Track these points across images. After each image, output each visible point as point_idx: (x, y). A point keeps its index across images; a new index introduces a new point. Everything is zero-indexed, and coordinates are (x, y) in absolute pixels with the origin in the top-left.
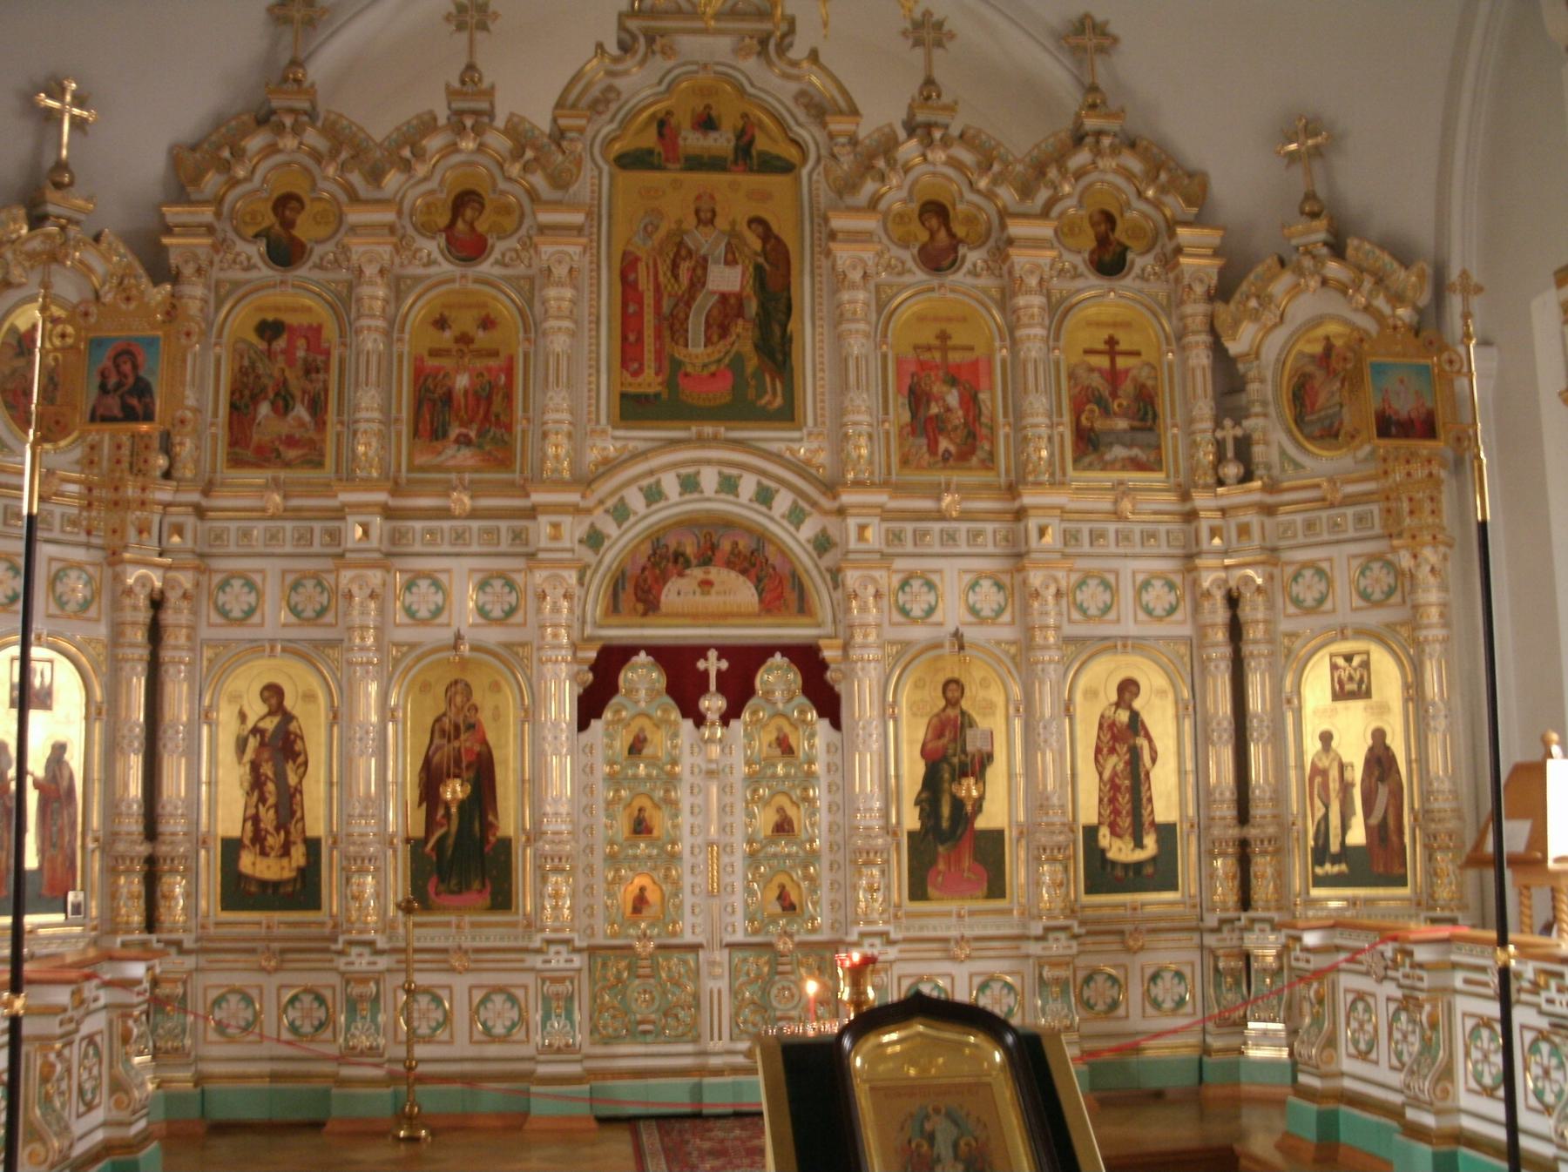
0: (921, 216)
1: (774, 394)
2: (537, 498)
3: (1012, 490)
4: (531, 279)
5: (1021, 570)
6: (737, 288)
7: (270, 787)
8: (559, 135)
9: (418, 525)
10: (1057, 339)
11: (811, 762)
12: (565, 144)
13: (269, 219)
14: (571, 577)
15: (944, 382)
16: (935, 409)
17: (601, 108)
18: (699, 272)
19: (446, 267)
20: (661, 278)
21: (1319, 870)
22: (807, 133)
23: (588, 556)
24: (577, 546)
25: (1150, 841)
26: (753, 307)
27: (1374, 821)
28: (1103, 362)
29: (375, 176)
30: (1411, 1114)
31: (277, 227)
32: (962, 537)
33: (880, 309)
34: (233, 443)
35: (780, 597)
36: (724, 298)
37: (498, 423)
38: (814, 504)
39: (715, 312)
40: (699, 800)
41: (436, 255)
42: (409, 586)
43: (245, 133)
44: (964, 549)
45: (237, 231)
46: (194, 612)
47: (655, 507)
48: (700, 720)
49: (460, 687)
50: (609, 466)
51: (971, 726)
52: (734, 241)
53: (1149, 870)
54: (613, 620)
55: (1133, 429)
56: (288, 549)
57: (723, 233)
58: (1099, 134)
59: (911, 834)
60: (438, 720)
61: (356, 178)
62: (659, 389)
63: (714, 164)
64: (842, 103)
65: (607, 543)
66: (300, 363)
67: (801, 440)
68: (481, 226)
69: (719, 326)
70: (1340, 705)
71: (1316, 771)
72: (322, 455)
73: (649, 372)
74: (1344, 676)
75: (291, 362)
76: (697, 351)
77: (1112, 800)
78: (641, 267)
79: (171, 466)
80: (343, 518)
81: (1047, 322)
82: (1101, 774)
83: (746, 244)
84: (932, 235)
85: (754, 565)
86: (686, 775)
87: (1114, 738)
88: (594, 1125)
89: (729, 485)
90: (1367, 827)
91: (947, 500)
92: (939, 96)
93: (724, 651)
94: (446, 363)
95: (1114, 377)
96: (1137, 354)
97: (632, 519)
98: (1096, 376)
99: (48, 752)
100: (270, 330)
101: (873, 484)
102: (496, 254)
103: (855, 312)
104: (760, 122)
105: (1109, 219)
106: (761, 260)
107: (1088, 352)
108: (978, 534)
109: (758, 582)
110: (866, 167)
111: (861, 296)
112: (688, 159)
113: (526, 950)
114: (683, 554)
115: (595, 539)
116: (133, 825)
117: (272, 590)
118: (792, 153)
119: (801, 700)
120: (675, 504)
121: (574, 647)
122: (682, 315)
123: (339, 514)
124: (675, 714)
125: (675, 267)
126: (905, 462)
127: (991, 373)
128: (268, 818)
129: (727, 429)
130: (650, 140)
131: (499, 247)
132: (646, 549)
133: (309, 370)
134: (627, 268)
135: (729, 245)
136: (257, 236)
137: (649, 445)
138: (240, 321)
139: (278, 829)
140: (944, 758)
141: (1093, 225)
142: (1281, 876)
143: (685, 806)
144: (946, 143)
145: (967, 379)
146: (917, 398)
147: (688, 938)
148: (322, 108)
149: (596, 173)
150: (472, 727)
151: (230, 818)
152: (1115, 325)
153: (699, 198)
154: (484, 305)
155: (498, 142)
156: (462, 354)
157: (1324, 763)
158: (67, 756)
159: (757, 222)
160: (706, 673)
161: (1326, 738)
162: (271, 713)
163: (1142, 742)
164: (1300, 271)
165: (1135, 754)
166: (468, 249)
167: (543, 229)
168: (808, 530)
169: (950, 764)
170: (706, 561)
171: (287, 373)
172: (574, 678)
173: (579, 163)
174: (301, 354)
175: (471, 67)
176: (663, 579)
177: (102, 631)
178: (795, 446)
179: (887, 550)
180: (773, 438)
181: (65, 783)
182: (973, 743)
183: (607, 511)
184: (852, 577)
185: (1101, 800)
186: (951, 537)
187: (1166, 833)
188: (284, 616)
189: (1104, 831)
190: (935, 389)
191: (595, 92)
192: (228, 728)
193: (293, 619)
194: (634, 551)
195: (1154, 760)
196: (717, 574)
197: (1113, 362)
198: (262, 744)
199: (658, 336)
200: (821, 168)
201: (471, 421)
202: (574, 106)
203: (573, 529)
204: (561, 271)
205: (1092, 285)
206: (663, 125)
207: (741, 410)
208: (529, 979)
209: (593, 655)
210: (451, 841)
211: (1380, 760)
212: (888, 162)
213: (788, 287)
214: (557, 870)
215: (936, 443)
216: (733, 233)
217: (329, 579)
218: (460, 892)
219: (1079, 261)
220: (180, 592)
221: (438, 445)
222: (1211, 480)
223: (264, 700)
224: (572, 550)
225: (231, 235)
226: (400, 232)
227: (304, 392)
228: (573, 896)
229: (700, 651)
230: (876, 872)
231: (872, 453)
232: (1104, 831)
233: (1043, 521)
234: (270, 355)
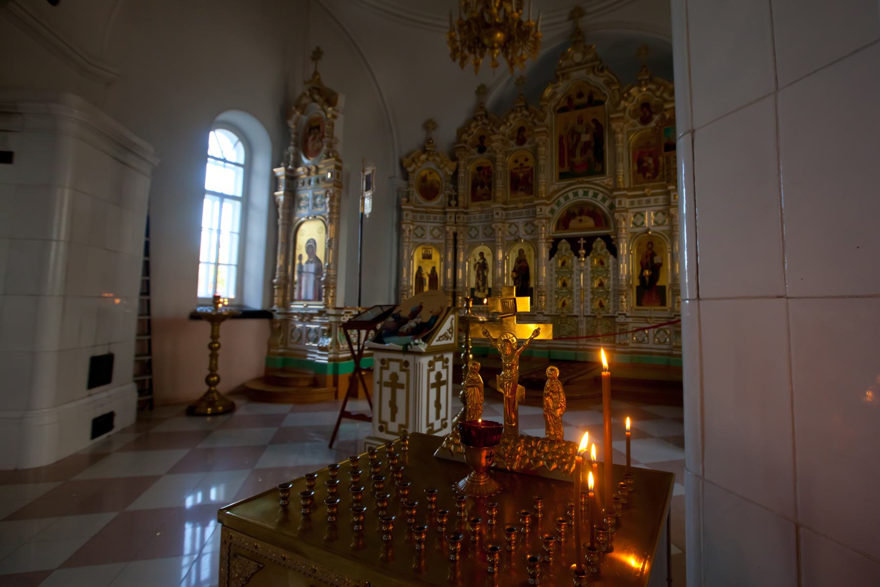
5: (668, 210)
7: (481, 276)
9: (511, 212)
11: (608, 267)
16: (645, 165)
26: (593, 144)
32: (652, 201)
42: (510, 227)
47: (567, 201)
48: (578, 256)
50: (555, 192)
61: (536, 121)
65: (555, 212)
67: (604, 179)
69: (584, 151)
76: (578, 159)
89: (586, 193)
91: (646, 190)
93: (585, 238)
94: (518, 171)
97: (561, 205)
102: (528, 142)
115: (552, 211)
116: (450, 285)
121: (547, 239)
124: (573, 255)
128: (480, 283)
131: (529, 140)
132: (565, 213)
134: (561, 138)
137: (565, 185)
138: (472, 168)
146: (640, 162)
147: (575, 313)
150: (525, 261)
151: (473, 285)
160: (580, 244)
162: (481, 259)
166: (521, 141)
168: (607, 203)
172: (548, 247)
173: (546, 114)
174: (486, 173)
176: (569, 220)
178: (603, 181)
180: (597, 180)
186: (648, 201)
190: (646, 158)
196: (584, 218)
203: (548, 209)
204: (541, 143)
206: (569, 99)
228: (545, 301)
229: (579, 238)
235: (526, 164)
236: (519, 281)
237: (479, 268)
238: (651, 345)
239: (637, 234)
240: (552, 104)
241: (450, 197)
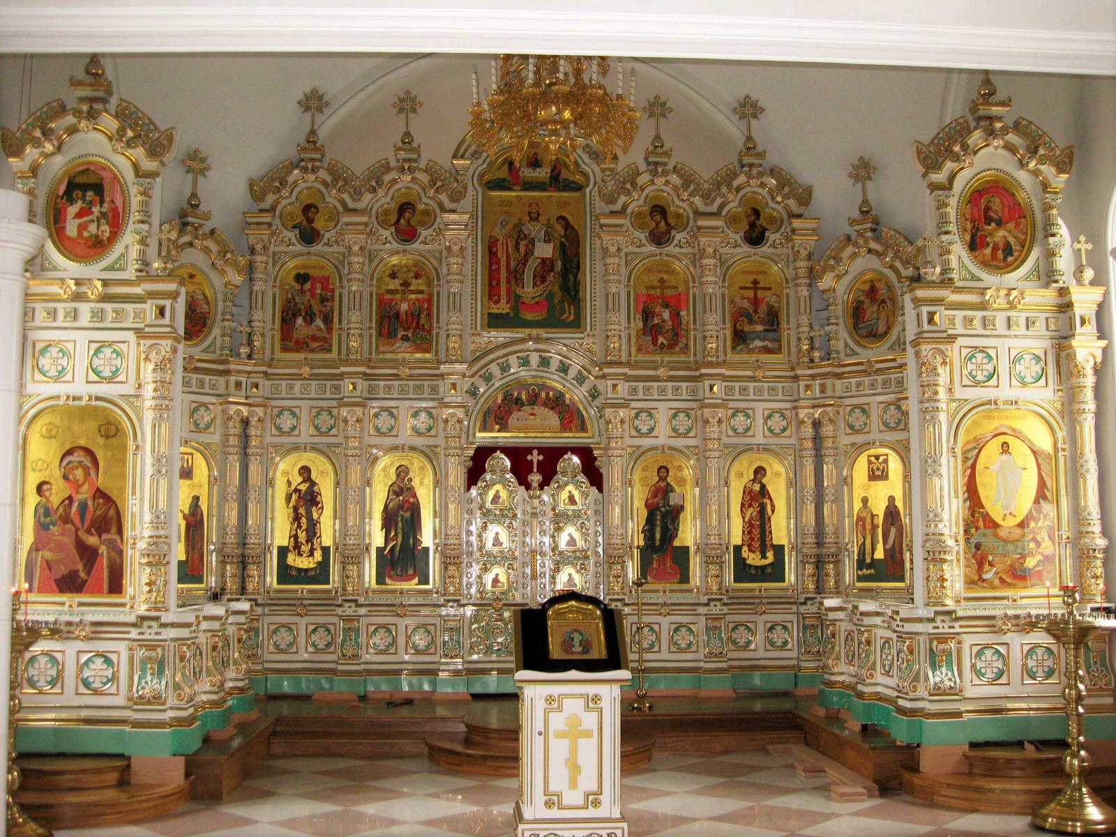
0: (651, 214)
1: (570, 314)
6: (550, 256)
7: (304, 520)
9: (382, 383)
10: (724, 281)
13: (300, 219)
15: (662, 306)
16: (656, 321)
18: (530, 247)
20: (510, 251)
21: (860, 572)
22: (591, 168)
25: (770, 555)
26: (559, 265)
27: (888, 547)
28: (750, 293)
30: (901, 702)
31: (304, 222)
32: (669, 391)
34: (283, 339)
36: (544, 261)
39: (538, 269)
44: (670, 397)
45: (283, 225)
46: (263, 429)
48: (528, 487)
51: (672, 491)
52: (549, 230)
53: (769, 570)
55: (766, 330)
58: (751, 165)
62: (508, 311)
69: (540, 277)
70: (872, 483)
71: (860, 519)
72: (331, 346)
73: (503, 301)
74: (875, 467)
76: (529, 291)
77: (750, 532)
78: (499, 244)
81: (719, 272)
82: (744, 518)
83: (556, 232)
84: (657, 224)
87: (752, 499)
88: (470, 698)
90: (884, 549)
92: (662, 146)
93: (542, 450)
95: (756, 302)
96: (770, 289)
98: (745, 301)
105: (756, 213)
106: (563, 240)
107: (741, 288)
110: (621, 189)
112: (525, 184)
122: (521, 271)
123: (341, 376)
125: (517, 244)
126: (639, 349)
127: (688, 302)
128: (302, 536)
130: (504, 173)
131: (424, 233)
133: (323, 300)
136: (294, 227)
139: (307, 542)
140: (658, 508)
141: (747, 217)
142: (839, 575)
144: (665, 173)
145: (675, 304)
146: (647, 315)
149: (475, 193)
152: (757, 273)
153: (530, 205)
156: (404, 292)
157: (864, 514)
161: (865, 501)
162: (304, 481)
163: (767, 501)
164: (856, 244)
165: (762, 508)
171: (312, 301)
173: (465, 188)
174: (318, 291)
175: (407, 134)
176: (509, 412)
178: (581, 341)
179: (627, 397)
181: (199, 517)
182: (674, 500)
183: (480, 376)
185: (743, 532)
187: (779, 550)
188: (312, 431)
189: (745, 548)
190: (657, 310)
192: (280, 490)
193: (315, 433)
195: (773, 511)
196: (538, 409)
197: (756, 294)
198: (299, 497)
199: (508, 282)
200: (596, 188)
201: (409, 328)
205: (746, 249)
207: (553, 321)
209: (471, 452)
211: (892, 514)
213: (578, 255)
215: (657, 340)
216: (549, 226)
217: (335, 411)
218: (402, 576)
219: (737, 237)
220: (256, 419)
221: (392, 341)
222: (806, 360)
223: (300, 474)
225: (280, 227)
227: (321, 312)
229: (529, 450)
230: (619, 567)
231: (621, 345)
232: (745, 548)
233: (713, 382)
234: (302, 292)
236: (396, 535)
237: (297, 501)
238: (664, 655)
239: (642, 450)
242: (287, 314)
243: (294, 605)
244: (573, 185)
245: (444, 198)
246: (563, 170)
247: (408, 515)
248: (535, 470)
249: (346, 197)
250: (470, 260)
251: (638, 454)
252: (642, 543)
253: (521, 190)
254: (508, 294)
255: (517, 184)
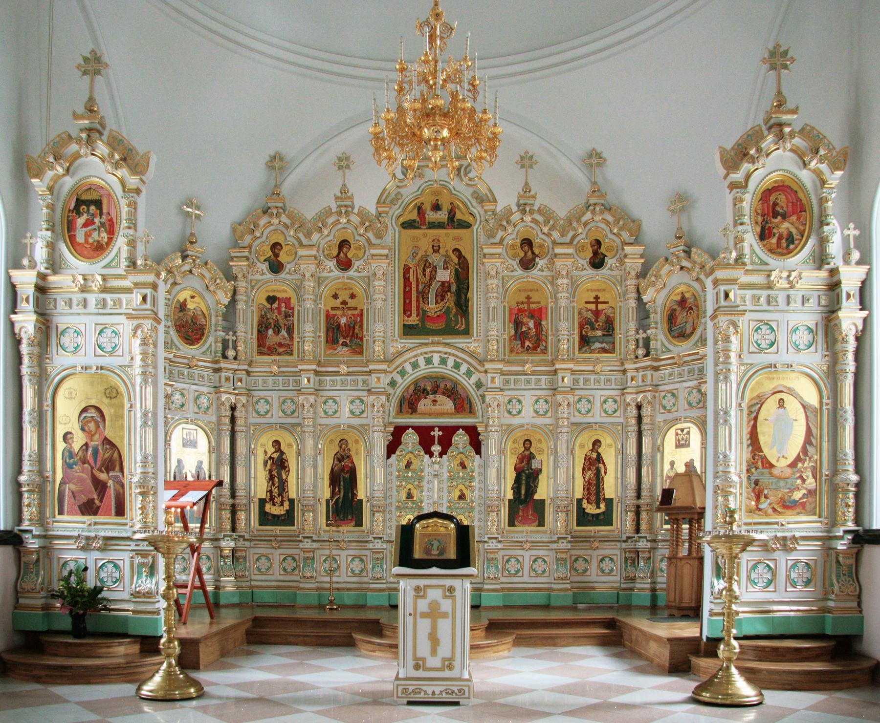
1: (462, 324)
2: (372, 367)
3: (553, 364)
4: (369, 277)
7: (276, 479)
8: (379, 214)
9: (328, 378)
11: (473, 472)
12: (381, 219)
13: (270, 254)
14: (383, 398)
16: (524, 329)
17: (395, 202)
19: (337, 273)
22: (477, 209)
23: (391, 391)
24: (387, 387)
26: (454, 287)
29: (308, 235)
31: (272, 257)
33: (503, 287)
35: (462, 407)
36: (443, 283)
37: (357, 337)
38: (475, 368)
39: (439, 290)
40: (431, 486)
41: (333, 268)
43: (259, 218)
44: (533, 387)
48: (431, 455)
49: (344, 441)
50: (400, 354)
52: (447, 259)
54: (401, 415)
56: (281, 387)
57: (442, 255)
59: (510, 501)
60: (336, 454)
63: (439, 225)
64: (491, 198)
66: (283, 313)
68: (350, 255)
73: (414, 315)
75: (280, 313)
76: (432, 307)
78: (411, 271)
79: (237, 355)
80: (300, 376)
85: (453, 394)
86: (426, 476)
89: (443, 361)
93: (441, 428)
94: (338, 312)
99: (196, 464)
100: (271, 299)
101: (498, 361)
103: (493, 289)
104: (458, 205)
108: (539, 380)
109: (454, 401)
111: (495, 281)
112: (430, 223)
113: (368, 542)
114: (426, 390)
115: (393, 384)
117: (275, 405)
118: (470, 219)
119: (469, 448)
120: (423, 370)
122: (427, 292)
123: (299, 373)
124: (422, 453)
125: (424, 270)
126: (512, 351)
128: (275, 491)
129: (443, 339)
131: (356, 264)
132: (412, 388)
133: (287, 316)
134: (407, 270)
135: (445, 261)
139: (279, 496)
140: (523, 471)
143: (425, 489)
144: (531, 212)
146: (517, 324)
148: (288, 205)
149: (393, 232)
153: (433, 241)
154: (351, 289)
155: (355, 219)
158: (203, 466)
159: (456, 250)
162: (276, 452)
167: (373, 255)
168: (474, 379)
169: (525, 473)
170: (435, 392)
172: (385, 438)
174: (283, 309)
175: (344, 185)
176: (418, 400)
177: (214, 419)
178: (469, 345)
179: (503, 387)
180: (460, 341)
183: (397, 372)
184: (488, 398)
186: (528, 382)
188: (281, 414)
190: (525, 320)
191: (393, 196)
194: (408, 387)
196: (440, 398)
198: (273, 463)
199: (418, 301)
200: (481, 226)
201: (347, 336)
202: (384, 202)
203: (386, 379)
204: (379, 274)
206: (420, 209)
207: (450, 331)
208: (367, 553)
210: (341, 500)
212: (507, 222)
213: (468, 279)
214: (378, 511)
215: (524, 343)
216: (447, 256)
218: (344, 520)
223: (274, 446)
224: (384, 388)
225: (256, 261)
226: (319, 258)
227: (285, 325)
229: (432, 428)
230: (495, 514)
231: (498, 348)
234: (272, 309)
235: (351, 303)
240: (396, 211)
241: (225, 344)
242: (262, 327)
243: (270, 541)
244: (465, 224)
245: (370, 235)
246: (457, 211)
247: (347, 476)
248: (436, 443)
249: (301, 235)
250: (390, 284)
251: (509, 430)
252: (511, 497)
253: (427, 228)
254: (418, 308)
255: (424, 224)
